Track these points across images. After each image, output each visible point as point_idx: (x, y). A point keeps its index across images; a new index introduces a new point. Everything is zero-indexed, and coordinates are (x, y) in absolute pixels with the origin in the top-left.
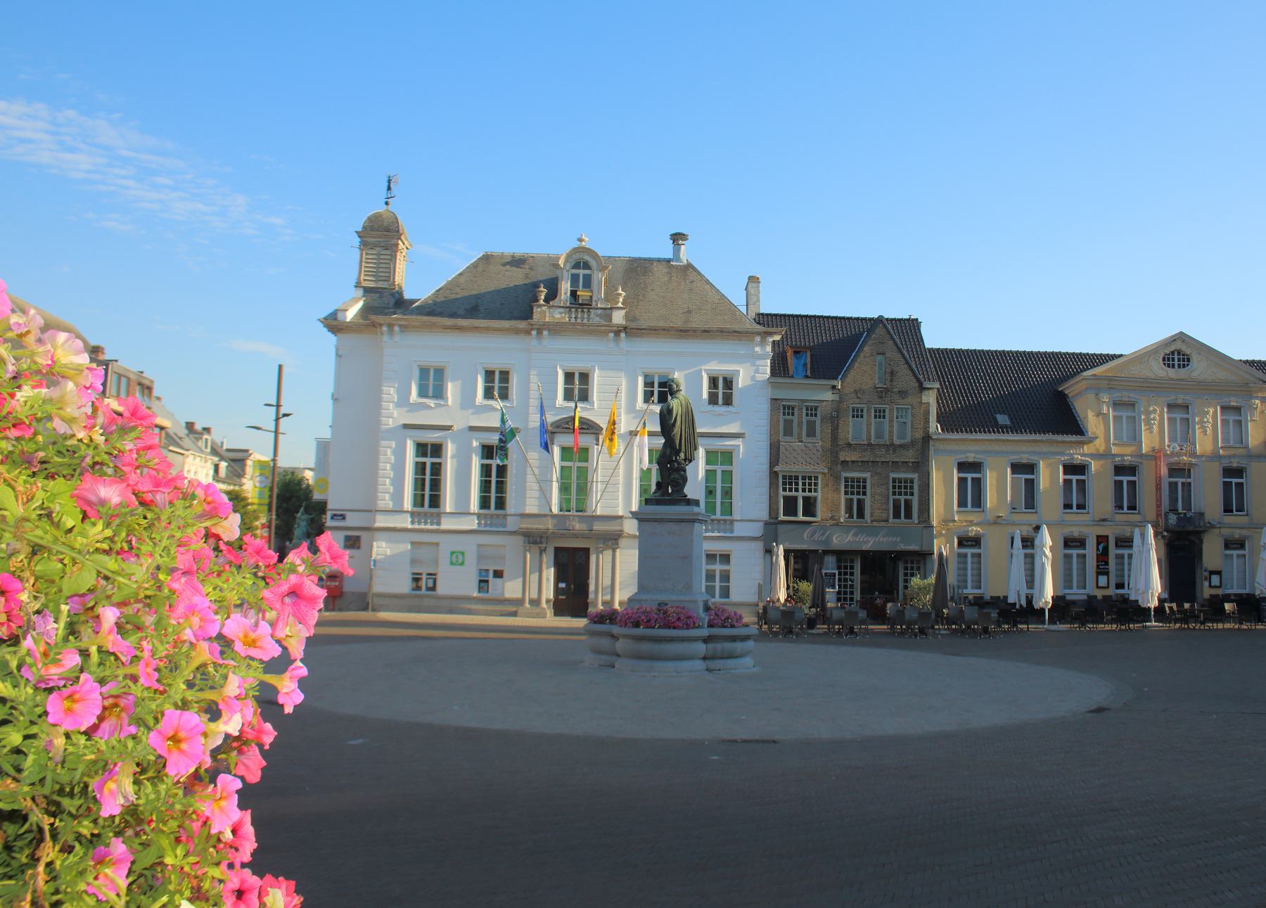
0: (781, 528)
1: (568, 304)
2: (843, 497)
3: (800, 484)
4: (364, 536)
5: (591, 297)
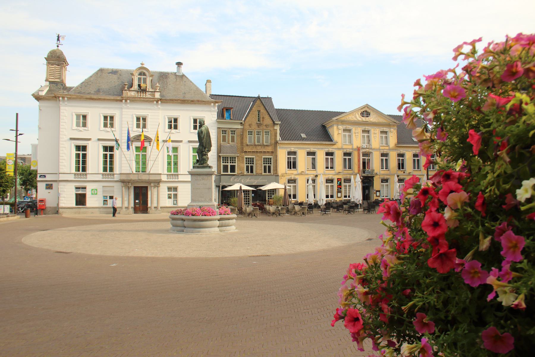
0: (222, 177)
1: (137, 90)
2: (245, 165)
3: (229, 160)
4: (54, 184)
5: (146, 87)
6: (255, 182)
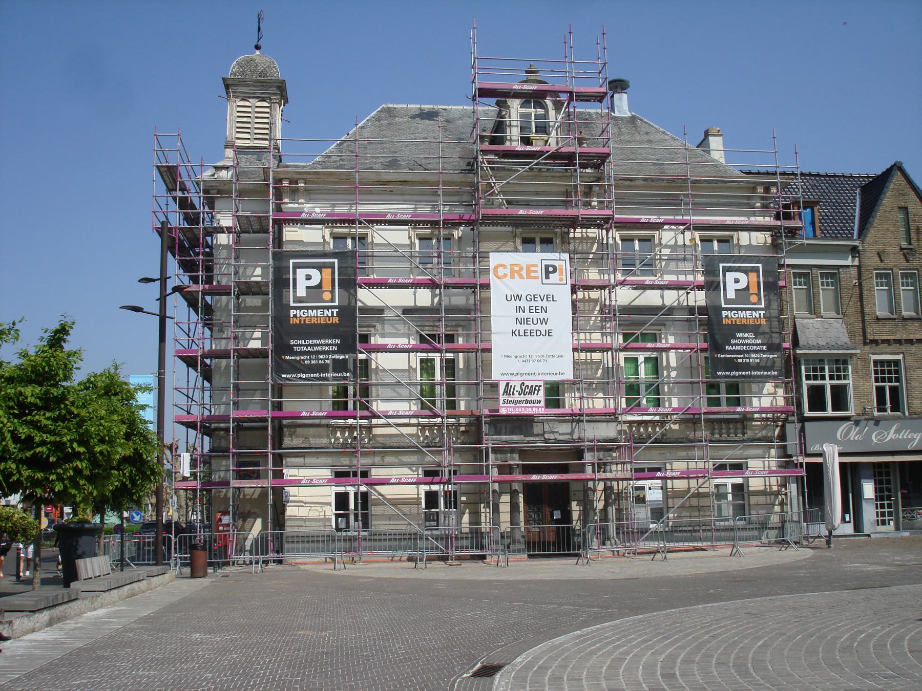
6: (914, 439)
